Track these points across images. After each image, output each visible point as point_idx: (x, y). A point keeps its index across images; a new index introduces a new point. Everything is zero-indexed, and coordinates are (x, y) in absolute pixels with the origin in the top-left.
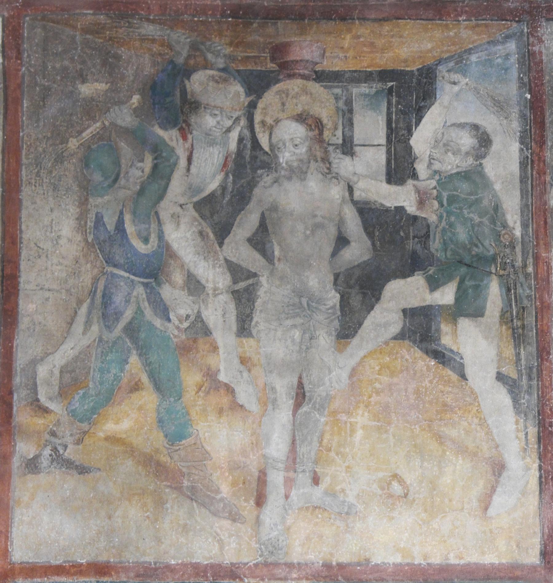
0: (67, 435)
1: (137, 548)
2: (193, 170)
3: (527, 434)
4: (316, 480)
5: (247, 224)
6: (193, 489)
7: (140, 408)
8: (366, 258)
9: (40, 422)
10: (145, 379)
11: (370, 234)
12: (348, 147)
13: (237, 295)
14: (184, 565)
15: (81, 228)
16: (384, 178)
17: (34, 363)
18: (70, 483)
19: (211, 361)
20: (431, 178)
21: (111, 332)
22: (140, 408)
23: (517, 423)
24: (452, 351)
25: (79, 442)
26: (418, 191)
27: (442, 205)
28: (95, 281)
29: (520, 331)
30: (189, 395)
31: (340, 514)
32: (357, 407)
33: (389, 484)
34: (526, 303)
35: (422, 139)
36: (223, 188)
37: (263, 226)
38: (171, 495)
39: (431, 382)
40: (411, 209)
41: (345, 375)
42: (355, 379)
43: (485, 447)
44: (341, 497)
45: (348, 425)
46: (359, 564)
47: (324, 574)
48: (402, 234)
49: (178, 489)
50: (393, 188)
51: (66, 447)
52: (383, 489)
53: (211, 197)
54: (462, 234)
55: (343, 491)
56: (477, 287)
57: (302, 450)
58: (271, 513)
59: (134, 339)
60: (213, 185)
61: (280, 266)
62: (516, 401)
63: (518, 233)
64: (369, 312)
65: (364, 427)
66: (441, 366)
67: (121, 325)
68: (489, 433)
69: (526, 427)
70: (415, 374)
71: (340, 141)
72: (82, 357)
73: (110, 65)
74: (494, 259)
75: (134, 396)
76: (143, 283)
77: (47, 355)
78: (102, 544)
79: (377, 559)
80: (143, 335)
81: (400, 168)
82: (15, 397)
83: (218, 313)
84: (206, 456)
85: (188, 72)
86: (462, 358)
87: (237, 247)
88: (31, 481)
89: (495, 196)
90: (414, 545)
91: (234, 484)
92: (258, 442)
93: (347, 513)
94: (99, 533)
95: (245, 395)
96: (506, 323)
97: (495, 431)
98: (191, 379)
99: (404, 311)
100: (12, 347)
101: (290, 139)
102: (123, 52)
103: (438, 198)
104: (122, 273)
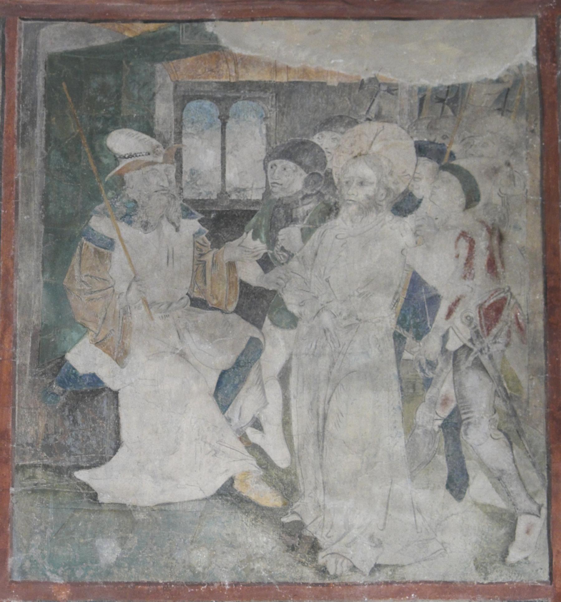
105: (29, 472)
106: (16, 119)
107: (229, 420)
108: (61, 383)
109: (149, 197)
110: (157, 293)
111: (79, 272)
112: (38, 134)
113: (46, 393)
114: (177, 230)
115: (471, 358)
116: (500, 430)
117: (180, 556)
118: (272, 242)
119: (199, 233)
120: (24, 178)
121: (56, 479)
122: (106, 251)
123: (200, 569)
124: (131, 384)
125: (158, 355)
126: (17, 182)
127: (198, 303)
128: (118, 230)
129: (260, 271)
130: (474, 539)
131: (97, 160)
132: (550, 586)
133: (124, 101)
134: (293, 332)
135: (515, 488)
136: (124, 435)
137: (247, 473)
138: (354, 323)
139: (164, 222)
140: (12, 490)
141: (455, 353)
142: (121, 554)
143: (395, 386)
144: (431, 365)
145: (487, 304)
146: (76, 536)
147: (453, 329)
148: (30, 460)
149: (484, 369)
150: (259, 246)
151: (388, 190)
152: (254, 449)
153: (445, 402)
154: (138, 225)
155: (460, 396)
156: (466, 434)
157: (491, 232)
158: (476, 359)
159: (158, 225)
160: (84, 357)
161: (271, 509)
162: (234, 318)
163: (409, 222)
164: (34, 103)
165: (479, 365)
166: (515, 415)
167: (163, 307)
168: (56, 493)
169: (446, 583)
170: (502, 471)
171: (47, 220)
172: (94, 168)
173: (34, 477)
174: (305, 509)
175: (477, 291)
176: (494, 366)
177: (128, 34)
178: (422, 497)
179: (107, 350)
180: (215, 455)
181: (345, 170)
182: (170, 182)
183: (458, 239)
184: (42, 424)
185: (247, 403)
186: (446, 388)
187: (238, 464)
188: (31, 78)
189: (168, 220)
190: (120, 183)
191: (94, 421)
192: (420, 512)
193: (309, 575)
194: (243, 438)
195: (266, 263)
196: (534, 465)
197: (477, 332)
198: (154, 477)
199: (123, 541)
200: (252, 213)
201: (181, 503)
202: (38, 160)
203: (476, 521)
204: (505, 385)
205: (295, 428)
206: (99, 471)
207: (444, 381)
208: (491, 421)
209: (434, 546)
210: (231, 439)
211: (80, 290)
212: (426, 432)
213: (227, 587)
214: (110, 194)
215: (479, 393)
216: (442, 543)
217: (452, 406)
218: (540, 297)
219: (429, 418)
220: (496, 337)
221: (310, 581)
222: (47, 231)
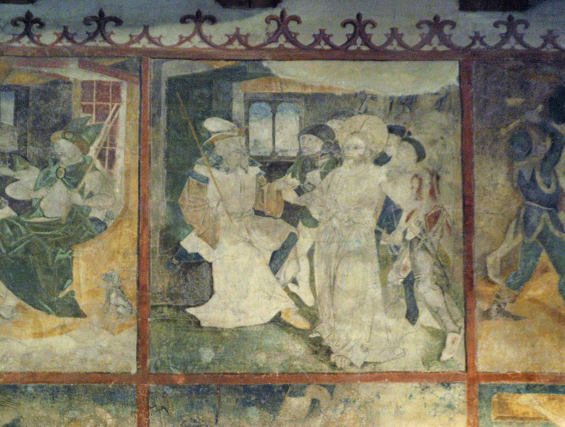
0: (506, 297)
1: (550, 364)
7: (549, 283)
9: (490, 290)
10: (550, 265)
15: (510, 178)
17: (485, 255)
18: (509, 326)
21: (530, 238)
22: (549, 283)
25: (513, 301)
28: (519, 208)
51: (505, 304)
59: (544, 243)
67: (535, 235)
72: (514, 251)
75: (545, 275)
77: (493, 251)
78: (530, 362)
80: (549, 240)
82: (475, 275)
94: (528, 355)
100: (471, 247)
104: (535, 205)
105: (159, 309)
106: (149, 111)
107: (278, 279)
108: (177, 258)
109: (230, 155)
110: (235, 207)
111: (188, 197)
112: (163, 120)
113: (169, 264)
114: (246, 172)
115: (420, 244)
117: (249, 357)
118: (303, 179)
119: (259, 174)
120: (154, 144)
121: (175, 313)
122: (203, 184)
123: (261, 365)
124: (220, 259)
125: (235, 242)
126: (150, 146)
127: (258, 213)
128: (211, 172)
129: (295, 195)
130: (422, 347)
131: (198, 134)
132: (465, 374)
133: (214, 102)
134: (315, 230)
135: (446, 317)
136: (216, 288)
137: (288, 309)
138: (352, 224)
139: (239, 169)
140: (149, 319)
141: (411, 242)
142: (215, 356)
143: (376, 260)
144: (397, 248)
145: (430, 214)
146: (188, 346)
147: (408, 228)
148: (159, 302)
150: (296, 182)
151: (371, 151)
152: (293, 295)
153: (405, 269)
154: (223, 169)
155: (414, 266)
156: (417, 287)
157: (432, 175)
158: (424, 244)
159: (235, 170)
160: (191, 243)
161: (303, 330)
162: (281, 221)
163: (384, 169)
164: (160, 103)
166: (446, 276)
167: (238, 215)
168: (175, 321)
169: (406, 372)
170: (438, 308)
171: (168, 167)
172: (196, 138)
173: (162, 312)
174: (323, 330)
175: (424, 207)
176: (434, 248)
177: (216, 67)
178: (391, 322)
179: (205, 240)
180: (270, 299)
181: (346, 140)
182: (242, 146)
183: (413, 177)
184: (166, 281)
185: (289, 269)
186: (405, 260)
187: (284, 304)
188: (158, 89)
189: (241, 167)
190: (211, 147)
191: (198, 279)
192: (390, 331)
193: (326, 368)
194: (286, 289)
195: (299, 191)
196: (457, 304)
197: (424, 230)
198: (234, 311)
199: (215, 349)
200: (290, 164)
201: (250, 326)
202: (162, 134)
204: (440, 259)
205: (317, 283)
206: (201, 308)
207: (404, 257)
208: (432, 280)
209: (399, 351)
210: (279, 290)
211: (188, 206)
212: (394, 286)
213: (278, 375)
214: (206, 153)
215: (425, 264)
216: (404, 350)
217: (409, 271)
218: (460, 210)
219: (396, 277)
220: (435, 232)
221: (327, 372)
222: (168, 173)
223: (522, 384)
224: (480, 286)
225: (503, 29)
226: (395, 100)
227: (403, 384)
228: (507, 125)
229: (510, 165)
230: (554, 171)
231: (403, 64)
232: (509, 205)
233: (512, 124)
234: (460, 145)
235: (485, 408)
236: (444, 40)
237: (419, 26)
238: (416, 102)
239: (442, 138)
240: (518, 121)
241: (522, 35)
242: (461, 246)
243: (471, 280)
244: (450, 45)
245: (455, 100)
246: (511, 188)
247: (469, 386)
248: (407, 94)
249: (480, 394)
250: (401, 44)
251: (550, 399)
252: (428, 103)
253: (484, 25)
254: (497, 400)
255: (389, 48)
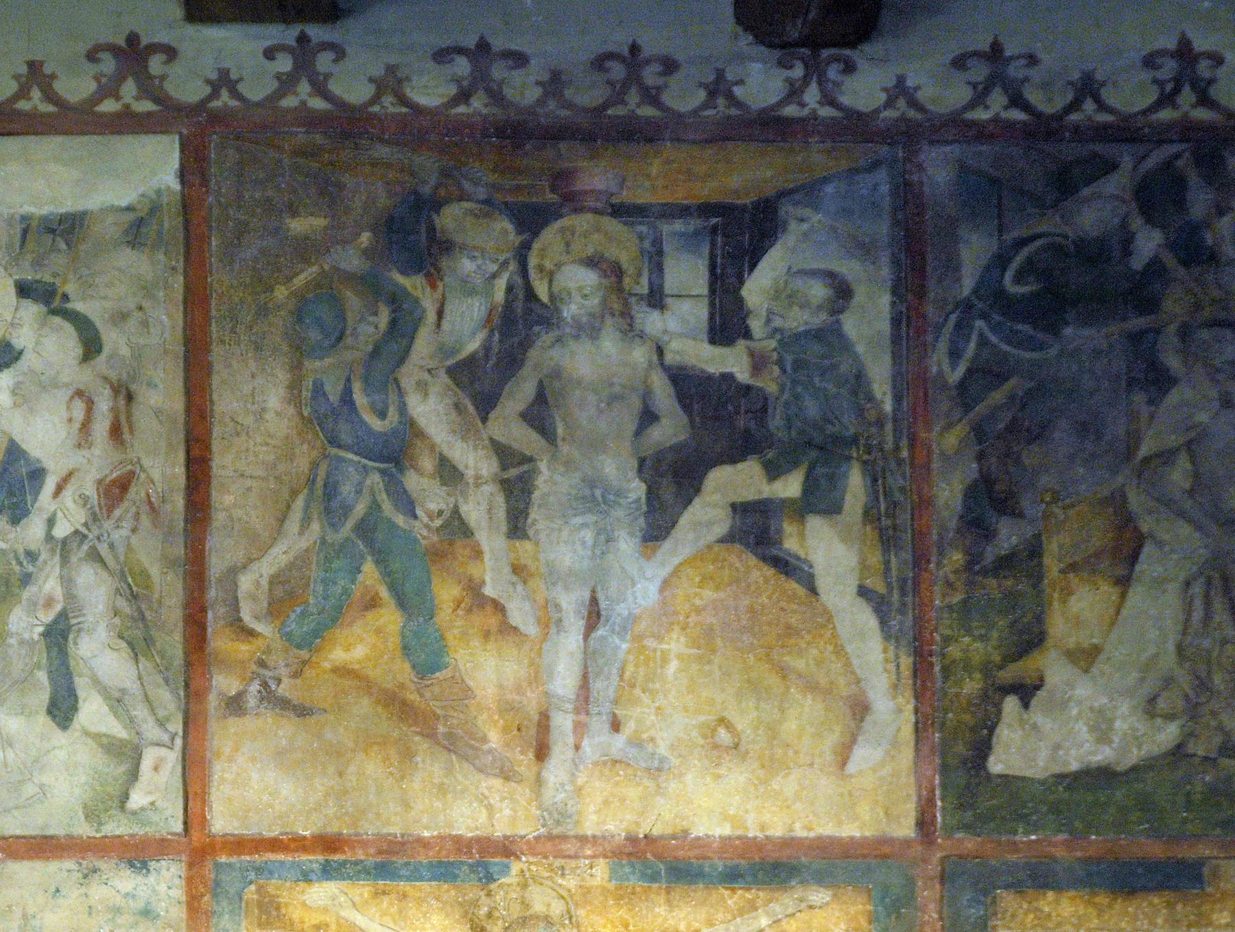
0: (280, 663)
1: (378, 814)
2: (446, 325)
3: (898, 666)
4: (616, 726)
5: (521, 393)
6: (450, 736)
7: (379, 631)
8: (682, 438)
10: (384, 593)
11: (686, 407)
12: (656, 299)
13: (507, 486)
14: (441, 838)
16: (705, 337)
17: (233, 572)
18: (285, 730)
19: (474, 570)
20: (771, 336)
21: (337, 531)
23: (885, 651)
24: (798, 558)
25: (296, 675)
26: (752, 354)
27: (784, 371)
28: (315, 465)
29: (891, 532)
30: (444, 614)
31: (648, 769)
32: (669, 630)
33: (714, 730)
34: (898, 496)
35: (757, 288)
36: (487, 348)
37: (541, 398)
38: (422, 745)
39: (770, 598)
40: (743, 375)
41: (653, 588)
42: (666, 593)
43: (842, 681)
44: (650, 748)
45: (659, 653)
46: (674, 837)
47: (627, 850)
48: (730, 408)
49: (431, 736)
50: (718, 351)
51: (279, 681)
52: (705, 737)
53: (471, 361)
54: (812, 408)
55: (652, 739)
56: (831, 478)
57: (597, 685)
58: (556, 771)
59: (370, 543)
60: (473, 345)
61: (565, 449)
62: (883, 623)
63: (888, 407)
64: (685, 507)
65: (680, 657)
66: (783, 577)
67: (350, 524)
68: (848, 664)
69: (897, 657)
70: (749, 586)
71: (646, 291)
72: (299, 563)
73: (329, 195)
74: (855, 440)
75: (370, 615)
76: (379, 470)
77: (251, 561)
78: (331, 811)
79: (698, 831)
80: (380, 536)
81: (727, 324)
82: (210, 615)
83: (482, 508)
84: (468, 693)
85: (437, 205)
86: (811, 567)
87: (507, 424)
88: (234, 725)
89: (856, 358)
90: (747, 811)
91: (505, 730)
92: (538, 675)
93: (657, 770)
94: (327, 795)
95: (520, 614)
96: (871, 522)
97: (855, 662)
98: (446, 593)
99: (734, 506)
100: (203, 550)
101: (578, 288)
102: (347, 179)
103: (780, 362)
104: (350, 456)
115: (85, 547)
116: (121, 637)
130: (83, 779)
141: (64, 542)
144: (32, 556)
145: (108, 480)
149: (104, 565)
153: (49, 602)
155: (70, 596)
156: (76, 644)
165: (95, 556)
166: (143, 618)
169: (45, 837)
170: (123, 691)
175: (97, 462)
176: (116, 558)
186: (50, 584)
192: (11, 745)
197: (94, 515)
203: (87, 756)
204: (130, 580)
207: (47, 577)
208: (110, 627)
209: (29, 790)
212: (22, 642)
215: (95, 590)
216: (41, 786)
217: (58, 607)
218: (180, 470)
220: (119, 519)
223: (314, 860)
224: (220, 641)
225: (284, 64)
226: (34, 223)
227: (38, 865)
228: (289, 279)
229: (296, 367)
230: (396, 380)
231: (53, 143)
232: (291, 458)
233: (302, 277)
234: (181, 323)
235: (227, 917)
236: (149, 88)
237: (92, 56)
238: (82, 226)
239: (141, 308)
240: (315, 269)
241: (328, 76)
242: (179, 550)
243: (203, 628)
244: (161, 99)
245: (171, 222)
246: (297, 419)
247: (191, 865)
248: (63, 210)
249: (217, 883)
250: (50, 96)
251: (377, 894)
252: (109, 228)
253: (242, 54)
254: (255, 897)
255: (23, 105)
